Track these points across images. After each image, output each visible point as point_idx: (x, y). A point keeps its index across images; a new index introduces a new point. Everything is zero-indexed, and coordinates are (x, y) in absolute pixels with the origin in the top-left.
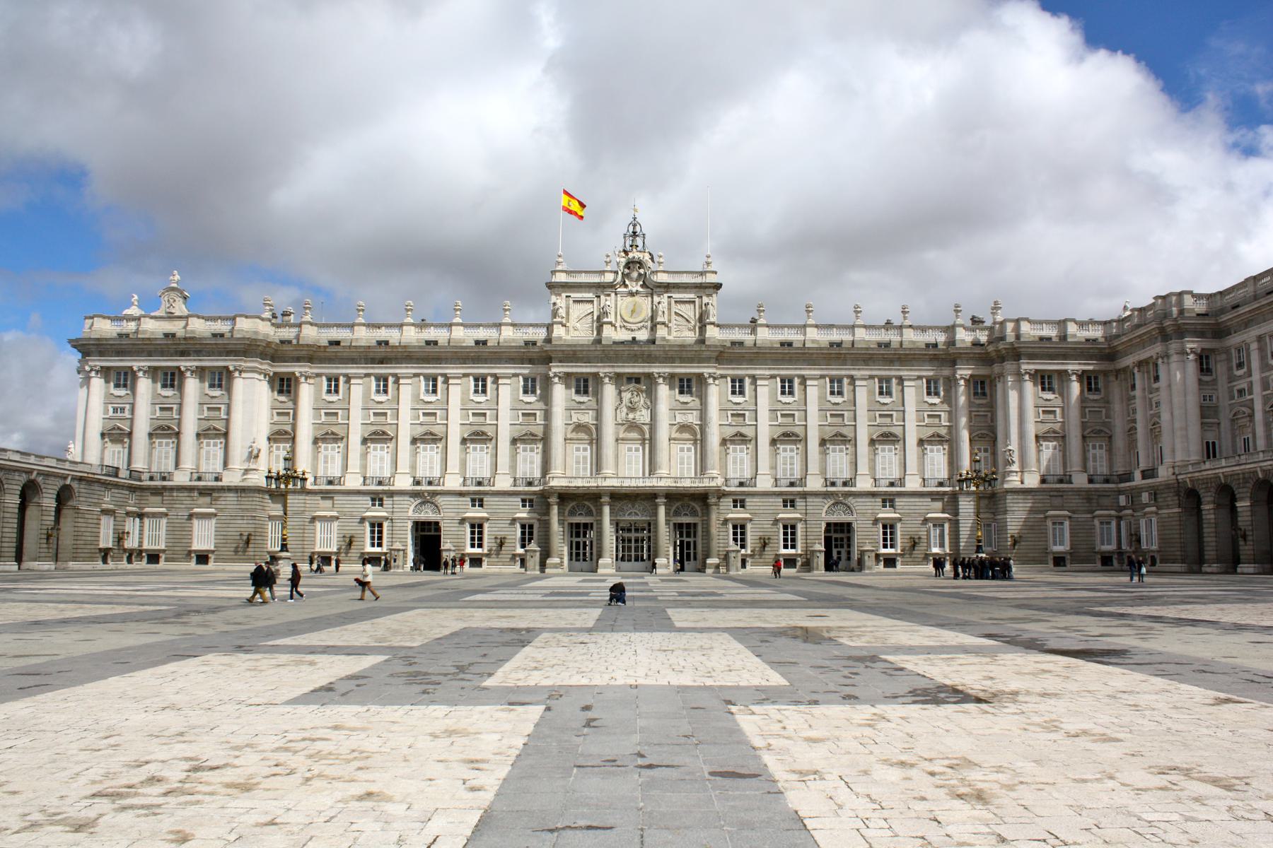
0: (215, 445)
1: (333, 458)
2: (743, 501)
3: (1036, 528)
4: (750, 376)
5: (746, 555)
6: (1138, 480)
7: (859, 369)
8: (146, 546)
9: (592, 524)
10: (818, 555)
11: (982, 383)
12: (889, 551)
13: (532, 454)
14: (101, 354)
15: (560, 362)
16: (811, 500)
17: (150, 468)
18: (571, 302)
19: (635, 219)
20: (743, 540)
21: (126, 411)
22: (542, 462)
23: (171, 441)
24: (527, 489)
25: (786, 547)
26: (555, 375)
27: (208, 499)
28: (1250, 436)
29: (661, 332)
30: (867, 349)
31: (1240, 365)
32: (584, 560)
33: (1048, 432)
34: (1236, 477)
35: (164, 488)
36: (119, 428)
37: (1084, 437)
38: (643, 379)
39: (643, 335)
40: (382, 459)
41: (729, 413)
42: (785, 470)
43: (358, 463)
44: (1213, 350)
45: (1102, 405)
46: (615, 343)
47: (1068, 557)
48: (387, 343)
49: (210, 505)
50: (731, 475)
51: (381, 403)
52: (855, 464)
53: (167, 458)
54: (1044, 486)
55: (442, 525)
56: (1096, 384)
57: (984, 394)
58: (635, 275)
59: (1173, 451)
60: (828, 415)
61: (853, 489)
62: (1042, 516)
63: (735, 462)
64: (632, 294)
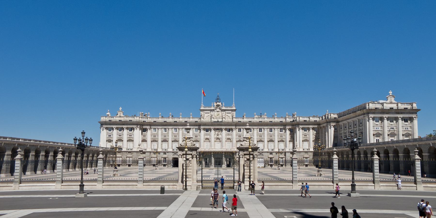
1: (155, 145)
4: (242, 128)
11: (292, 129)
14: (106, 124)
15: (203, 125)
19: (218, 95)
21: (111, 136)
26: (202, 128)
27: (130, 154)
29: (224, 119)
30: (267, 123)
33: (305, 140)
36: (110, 140)
39: (220, 120)
40: (166, 145)
41: (238, 136)
46: (214, 122)
48: (166, 122)
49: (131, 155)
51: (165, 134)
57: (292, 131)
61: (264, 151)
64: (218, 112)
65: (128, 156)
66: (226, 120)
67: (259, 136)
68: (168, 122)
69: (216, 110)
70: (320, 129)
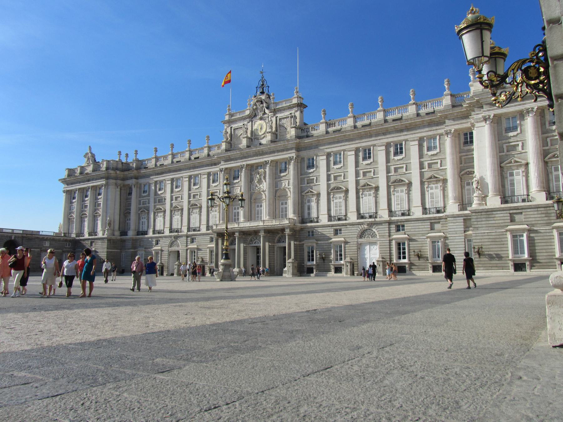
3: (497, 240)
7: (380, 139)
12: (403, 261)
16: (350, 229)
25: (337, 260)
37: (546, 163)
42: (336, 211)
54: (503, 206)
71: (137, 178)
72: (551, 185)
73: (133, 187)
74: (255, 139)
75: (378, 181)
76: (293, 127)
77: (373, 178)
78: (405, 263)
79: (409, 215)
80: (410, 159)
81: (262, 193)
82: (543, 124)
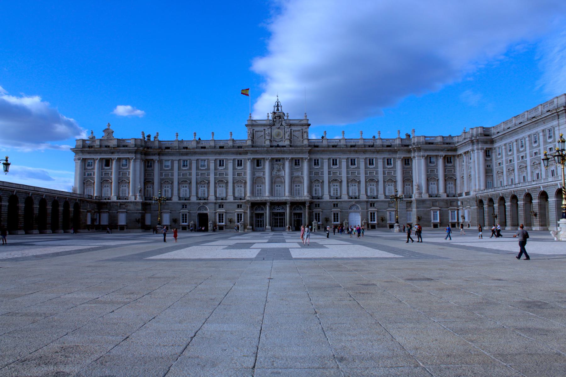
0: (125, 186)
1: (168, 191)
2: (319, 205)
5: (320, 224)
6: (464, 196)
8: (102, 223)
9: (263, 213)
10: (346, 224)
11: (408, 160)
12: (373, 222)
13: (241, 188)
15: (251, 154)
17: (101, 195)
18: (254, 132)
19: (278, 100)
20: (319, 219)
21: (92, 175)
22: (244, 191)
23: (109, 185)
24: (239, 201)
25: (335, 221)
28: (502, 180)
31: (499, 154)
32: (261, 227)
34: (494, 195)
35: (107, 202)
37: (445, 180)
38: (281, 160)
40: (186, 191)
43: (177, 192)
44: (490, 148)
45: (452, 168)
46: (271, 146)
47: (439, 224)
48: (186, 148)
49: (124, 209)
50: (314, 195)
52: (359, 190)
53: (107, 191)
54: (430, 198)
55: (209, 214)
56: (450, 160)
57: (408, 164)
58: (278, 121)
59: (476, 185)
60: (350, 172)
62: (429, 209)
63: (316, 190)
65: (119, 210)
66: (292, 144)
67: (350, 172)
68: (190, 149)
69: (274, 125)
70: (458, 157)
71: (159, 154)
72: (447, 190)
73: (156, 162)
74: (273, 141)
75: (360, 178)
76: (306, 139)
77: (356, 176)
78: (375, 224)
79: (377, 198)
80: (378, 169)
81: (282, 178)
82: (444, 163)
